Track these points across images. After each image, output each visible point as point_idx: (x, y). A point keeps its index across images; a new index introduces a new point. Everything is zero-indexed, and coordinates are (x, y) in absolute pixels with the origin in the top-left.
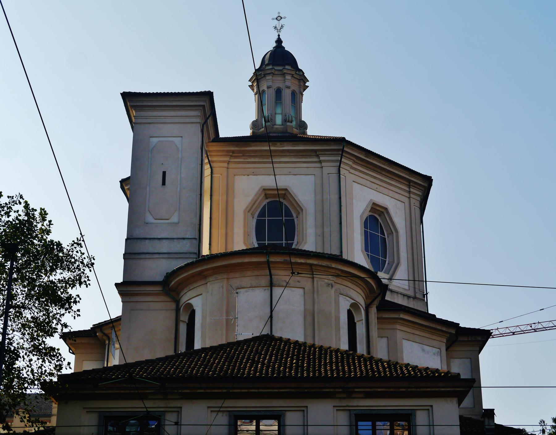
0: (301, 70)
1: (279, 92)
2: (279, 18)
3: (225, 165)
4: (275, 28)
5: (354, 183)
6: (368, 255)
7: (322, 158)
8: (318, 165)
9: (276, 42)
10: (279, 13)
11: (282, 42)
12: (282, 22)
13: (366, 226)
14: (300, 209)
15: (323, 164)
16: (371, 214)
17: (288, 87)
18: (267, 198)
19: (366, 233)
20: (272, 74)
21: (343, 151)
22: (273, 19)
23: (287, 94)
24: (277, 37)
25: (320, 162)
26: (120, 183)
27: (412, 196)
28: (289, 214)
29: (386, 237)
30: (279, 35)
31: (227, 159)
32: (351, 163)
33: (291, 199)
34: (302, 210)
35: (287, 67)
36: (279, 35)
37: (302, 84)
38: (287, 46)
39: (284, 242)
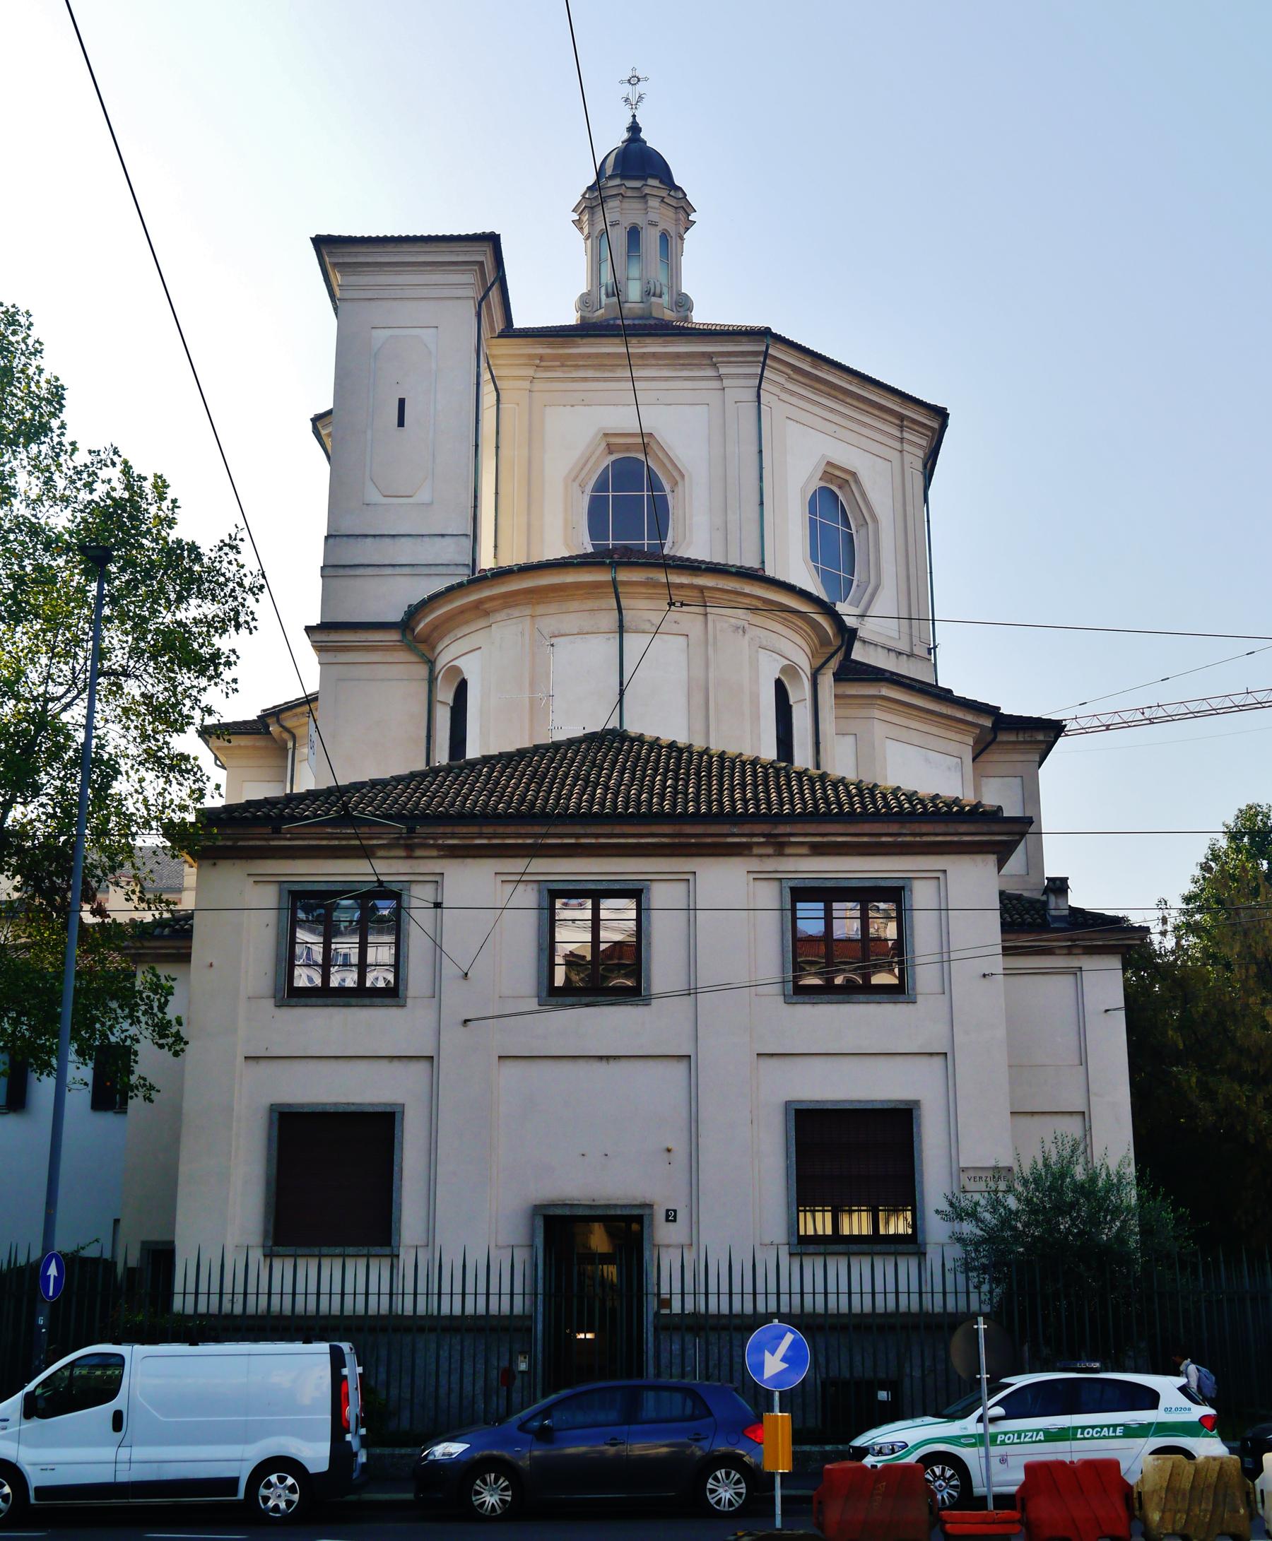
0: (679, 189)
1: (634, 234)
2: (634, 80)
3: (526, 384)
4: (627, 100)
5: (788, 421)
6: (817, 568)
7: (723, 370)
8: (716, 384)
9: (629, 129)
10: (634, 69)
11: (640, 130)
12: (641, 87)
13: (812, 510)
14: (678, 476)
15: (726, 382)
16: (823, 484)
17: (653, 224)
18: (611, 453)
19: (812, 523)
20: (620, 197)
21: (766, 354)
22: (622, 82)
23: (650, 239)
24: (631, 120)
25: (720, 378)
26: (310, 423)
27: (906, 447)
28: (654, 484)
29: (854, 531)
30: (634, 116)
31: (530, 372)
32: (781, 380)
33: (660, 454)
34: (683, 476)
35: (651, 182)
36: (634, 116)
37: (682, 215)
38: (651, 138)
39: (646, 542)
